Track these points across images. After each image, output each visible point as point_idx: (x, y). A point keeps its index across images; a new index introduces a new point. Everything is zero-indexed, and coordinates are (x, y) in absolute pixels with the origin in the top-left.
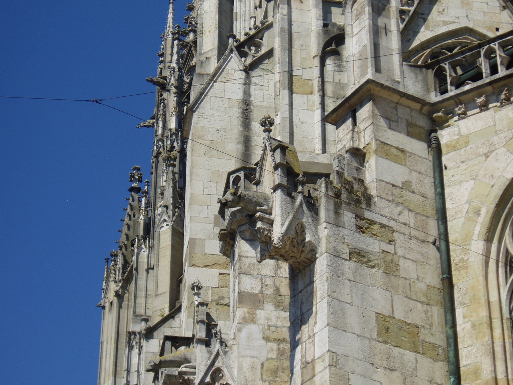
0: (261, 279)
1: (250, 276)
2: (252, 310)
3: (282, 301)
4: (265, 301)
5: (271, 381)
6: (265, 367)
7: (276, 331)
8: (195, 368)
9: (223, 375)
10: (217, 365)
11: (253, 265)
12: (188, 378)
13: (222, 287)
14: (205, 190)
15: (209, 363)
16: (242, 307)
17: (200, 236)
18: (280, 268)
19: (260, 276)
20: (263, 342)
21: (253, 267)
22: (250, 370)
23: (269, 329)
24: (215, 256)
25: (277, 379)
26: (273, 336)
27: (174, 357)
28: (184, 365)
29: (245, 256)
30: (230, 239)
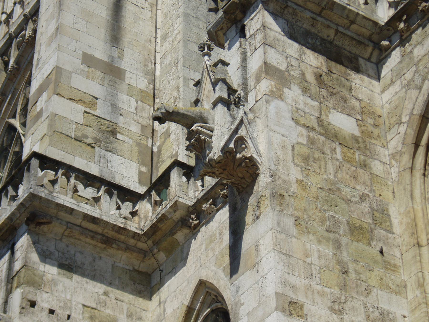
0: (287, 58)
1: (275, 50)
2: (279, 85)
3: (308, 88)
4: (291, 81)
5: (303, 167)
6: (296, 150)
7: (304, 117)
8: (212, 131)
9: (246, 147)
10: (242, 132)
11: (278, 40)
12: (205, 139)
13: (86, 126)
14: (74, 24)
15: (233, 127)
16: (269, 79)
17: (67, 67)
18: (305, 54)
19: (285, 54)
20: (292, 123)
21: (278, 42)
22: (281, 147)
23: (297, 112)
24: (81, 92)
25: (309, 168)
26: (302, 120)
27: (188, 111)
28: (199, 124)
29: (269, 27)
30: (241, 11)
